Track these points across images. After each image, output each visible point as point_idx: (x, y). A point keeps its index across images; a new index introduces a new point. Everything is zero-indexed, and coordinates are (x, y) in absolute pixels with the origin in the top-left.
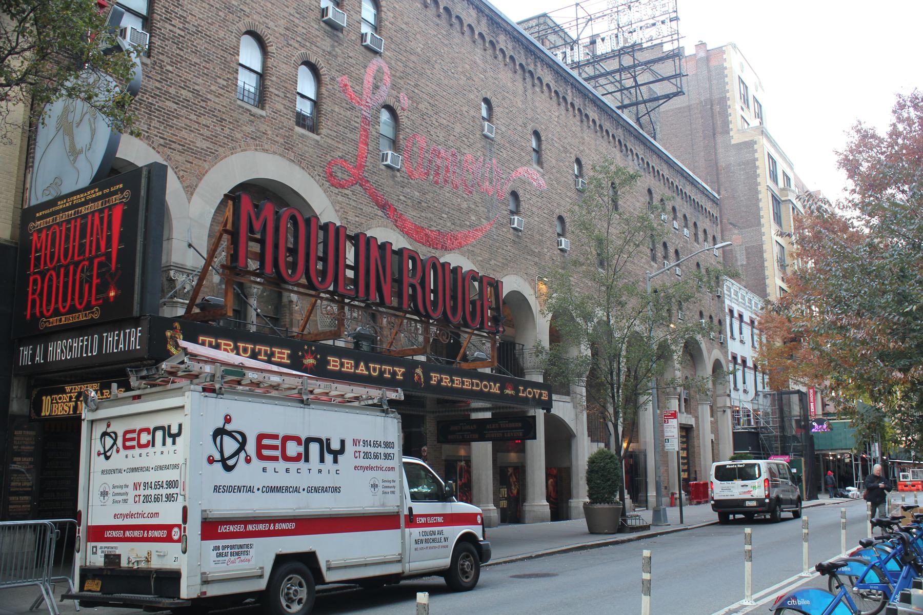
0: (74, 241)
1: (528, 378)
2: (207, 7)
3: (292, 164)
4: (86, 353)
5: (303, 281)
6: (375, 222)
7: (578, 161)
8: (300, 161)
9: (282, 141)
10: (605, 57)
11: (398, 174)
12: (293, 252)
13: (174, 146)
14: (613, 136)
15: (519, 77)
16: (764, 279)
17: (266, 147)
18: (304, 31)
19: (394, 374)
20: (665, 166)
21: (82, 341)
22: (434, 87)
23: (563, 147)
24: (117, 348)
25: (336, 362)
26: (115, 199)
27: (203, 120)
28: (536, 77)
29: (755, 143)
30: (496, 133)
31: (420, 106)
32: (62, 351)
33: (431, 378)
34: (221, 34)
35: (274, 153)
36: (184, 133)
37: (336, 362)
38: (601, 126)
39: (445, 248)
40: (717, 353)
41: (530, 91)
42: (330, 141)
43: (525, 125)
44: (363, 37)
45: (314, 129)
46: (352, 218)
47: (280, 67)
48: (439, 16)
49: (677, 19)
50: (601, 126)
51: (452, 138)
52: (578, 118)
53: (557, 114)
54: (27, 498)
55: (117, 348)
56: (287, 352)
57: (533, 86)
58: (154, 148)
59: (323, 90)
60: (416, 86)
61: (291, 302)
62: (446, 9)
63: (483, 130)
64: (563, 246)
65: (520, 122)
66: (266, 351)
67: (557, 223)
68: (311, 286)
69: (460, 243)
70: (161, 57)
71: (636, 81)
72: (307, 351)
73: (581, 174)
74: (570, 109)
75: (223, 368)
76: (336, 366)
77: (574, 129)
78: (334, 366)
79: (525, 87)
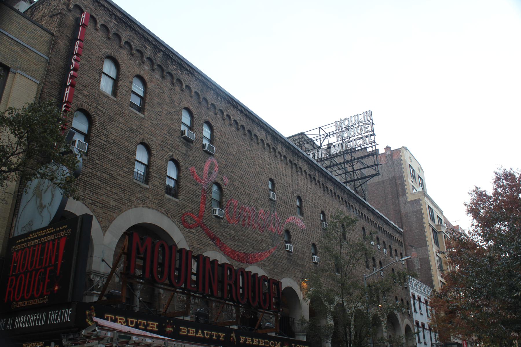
0: (37, 257)
1: (297, 338)
2: (120, 129)
4: (38, 323)
5: (167, 281)
7: (323, 213)
8: (167, 213)
9: (157, 202)
10: (336, 156)
11: (222, 221)
12: (161, 265)
13: (97, 204)
14: (342, 199)
15: (289, 167)
16: (431, 276)
17: (149, 205)
18: (172, 143)
19: (219, 337)
20: (371, 215)
21: (36, 316)
22: (242, 172)
23: (314, 205)
24: (56, 321)
25: (185, 329)
26: (62, 234)
27: (114, 190)
28: (298, 167)
29: (421, 200)
30: (277, 198)
31: (235, 183)
32: (23, 322)
33: (240, 339)
34: (127, 144)
35: (153, 209)
36: (103, 197)
37: (185, 329)
38: (335, 193)
39: (249, 263)
40: (407, 321)
41: (295, 174)
42: (184, 202)
43: (293, 193)
44: (204, 146)
45: (176, 195)
46: (196, 245)
47: (158, 162)
48: (245, 135)
49: (374, 135)
50: (335, 193)
51: (252, 200)
52: (322, 189)
53: (310, 187)
55: (56, 321)
56: (156, 324)
57: (297, 172)
58: (86, 205)
59: (181, 174)
60: (232, 172)
61: (160, 293)
62: (249, 131)
63: (270, 196)
64: (316, 261)
65: (290, 192)
66: (144, 323)
67: (312, 247)
68: (171, 285)
69: (257, 259)
70: (93, 156)
71: (353, 168)
73: (324, 220)
74: (318, 184)
75: (118, 334)
76: (185, 332)
77: (320, 195)
78: (183, 332)
79: (292, 173)
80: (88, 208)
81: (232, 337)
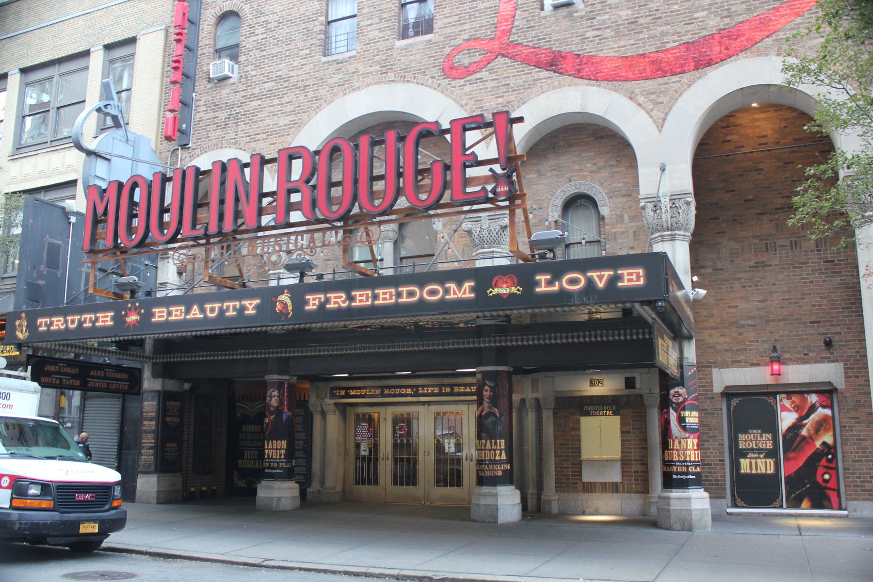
3: (393, 84)
6: (535, 90)
17: (357, 85)
19: (243, 308)
25: (163, 312)
33: (306, 302)
35: (368, 85)
36: (268, 121)
54: (152, 451)
66: (46, 322)
70: (246, 69)
72: (130, 309)
76: (163, 316)
81: (281, 302)
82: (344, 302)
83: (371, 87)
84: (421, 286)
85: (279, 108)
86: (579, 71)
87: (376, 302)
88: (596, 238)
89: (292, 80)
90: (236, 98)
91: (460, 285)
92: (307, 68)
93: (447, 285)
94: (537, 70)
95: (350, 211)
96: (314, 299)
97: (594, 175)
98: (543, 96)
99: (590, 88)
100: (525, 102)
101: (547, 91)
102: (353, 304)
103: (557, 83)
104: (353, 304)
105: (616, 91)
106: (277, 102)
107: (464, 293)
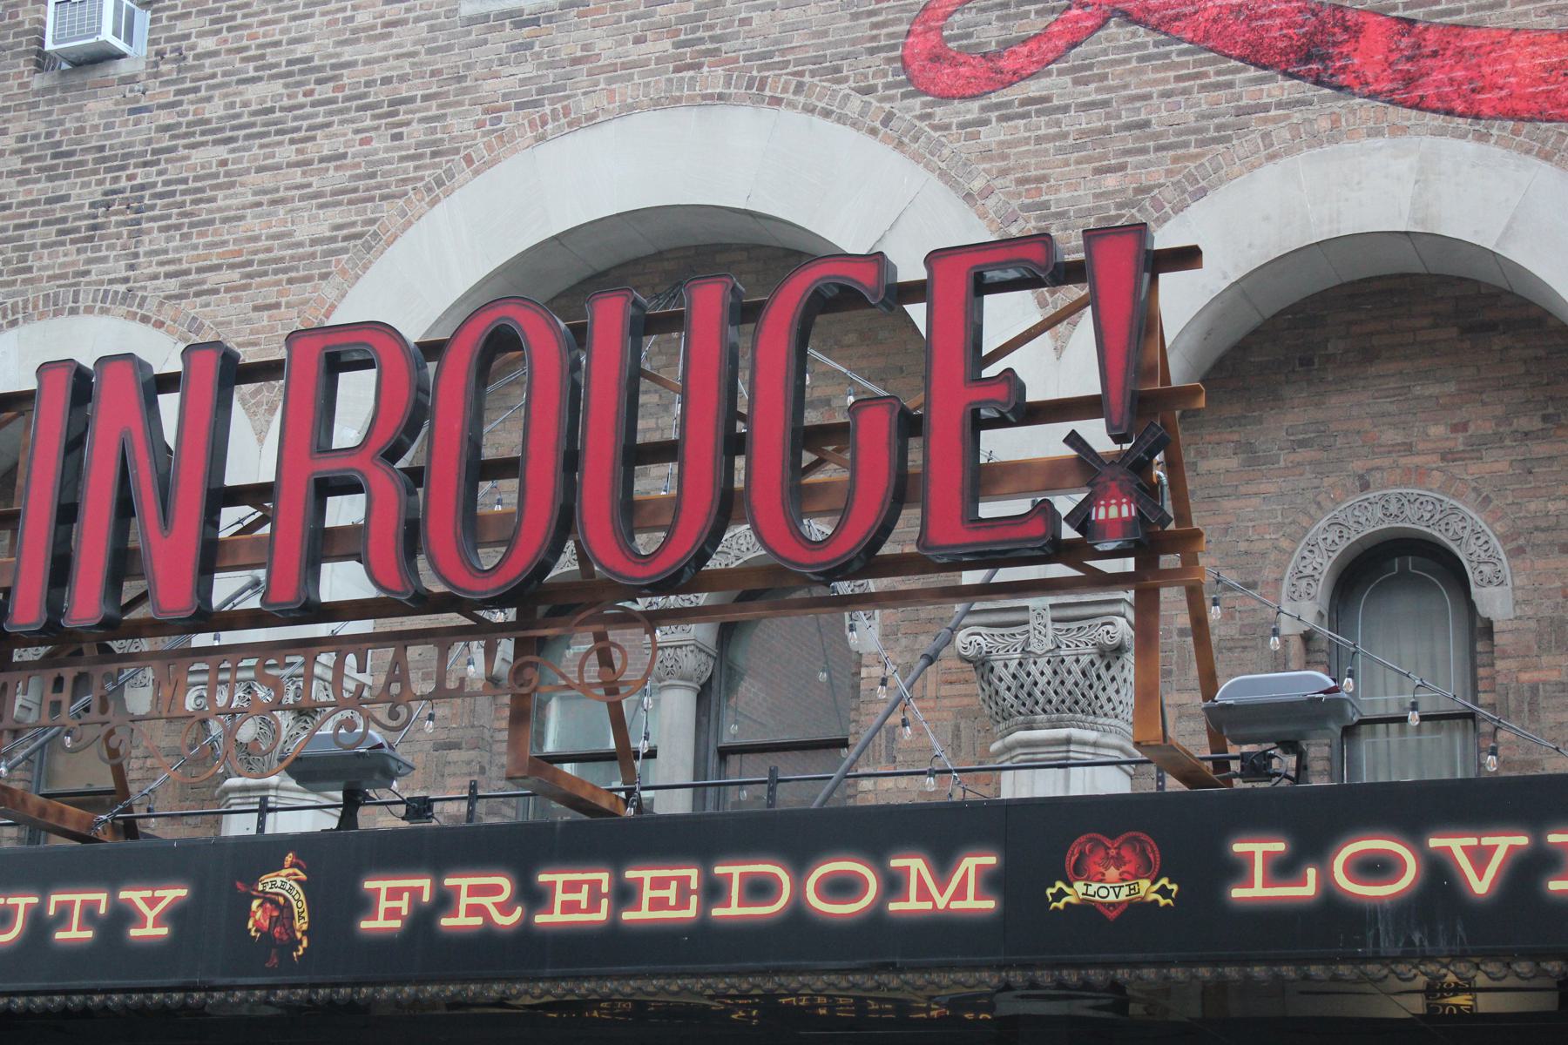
3: (719, 112)
6: (1240, 146)
17: (586, 106)
19: (123, 916)
33: (365, 905)
35: (629, 109)
36: (253, 223)
58: (145, 319)
70: (180, 27)
80: (159, 325)
81: (268, 899)
82: (505, 909)
83: (637, 119)
84: (800, 865)
85: (297, 176)
86: (1410, 80)
87: (627, 916)
88: (1462, 704)
89: (347, 76)
90: (135, 134)
91: (943, 864)
92: (405, 37)
93: (895, 863)
94: (1253, 72)
95: (545, 567)
96: (394, 894)
97: (1456, 469)
98: (1269, 171)
99: (1448, 144)
100: (1203, 192)
101: (1288, 152)
102: (540, 919)
103: (1324, 124)
104: (540, 919)
105: (1547, 157)
106: (287, 153)
107: (960, 894)
